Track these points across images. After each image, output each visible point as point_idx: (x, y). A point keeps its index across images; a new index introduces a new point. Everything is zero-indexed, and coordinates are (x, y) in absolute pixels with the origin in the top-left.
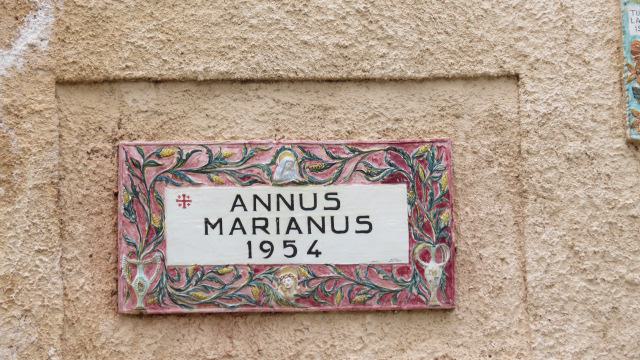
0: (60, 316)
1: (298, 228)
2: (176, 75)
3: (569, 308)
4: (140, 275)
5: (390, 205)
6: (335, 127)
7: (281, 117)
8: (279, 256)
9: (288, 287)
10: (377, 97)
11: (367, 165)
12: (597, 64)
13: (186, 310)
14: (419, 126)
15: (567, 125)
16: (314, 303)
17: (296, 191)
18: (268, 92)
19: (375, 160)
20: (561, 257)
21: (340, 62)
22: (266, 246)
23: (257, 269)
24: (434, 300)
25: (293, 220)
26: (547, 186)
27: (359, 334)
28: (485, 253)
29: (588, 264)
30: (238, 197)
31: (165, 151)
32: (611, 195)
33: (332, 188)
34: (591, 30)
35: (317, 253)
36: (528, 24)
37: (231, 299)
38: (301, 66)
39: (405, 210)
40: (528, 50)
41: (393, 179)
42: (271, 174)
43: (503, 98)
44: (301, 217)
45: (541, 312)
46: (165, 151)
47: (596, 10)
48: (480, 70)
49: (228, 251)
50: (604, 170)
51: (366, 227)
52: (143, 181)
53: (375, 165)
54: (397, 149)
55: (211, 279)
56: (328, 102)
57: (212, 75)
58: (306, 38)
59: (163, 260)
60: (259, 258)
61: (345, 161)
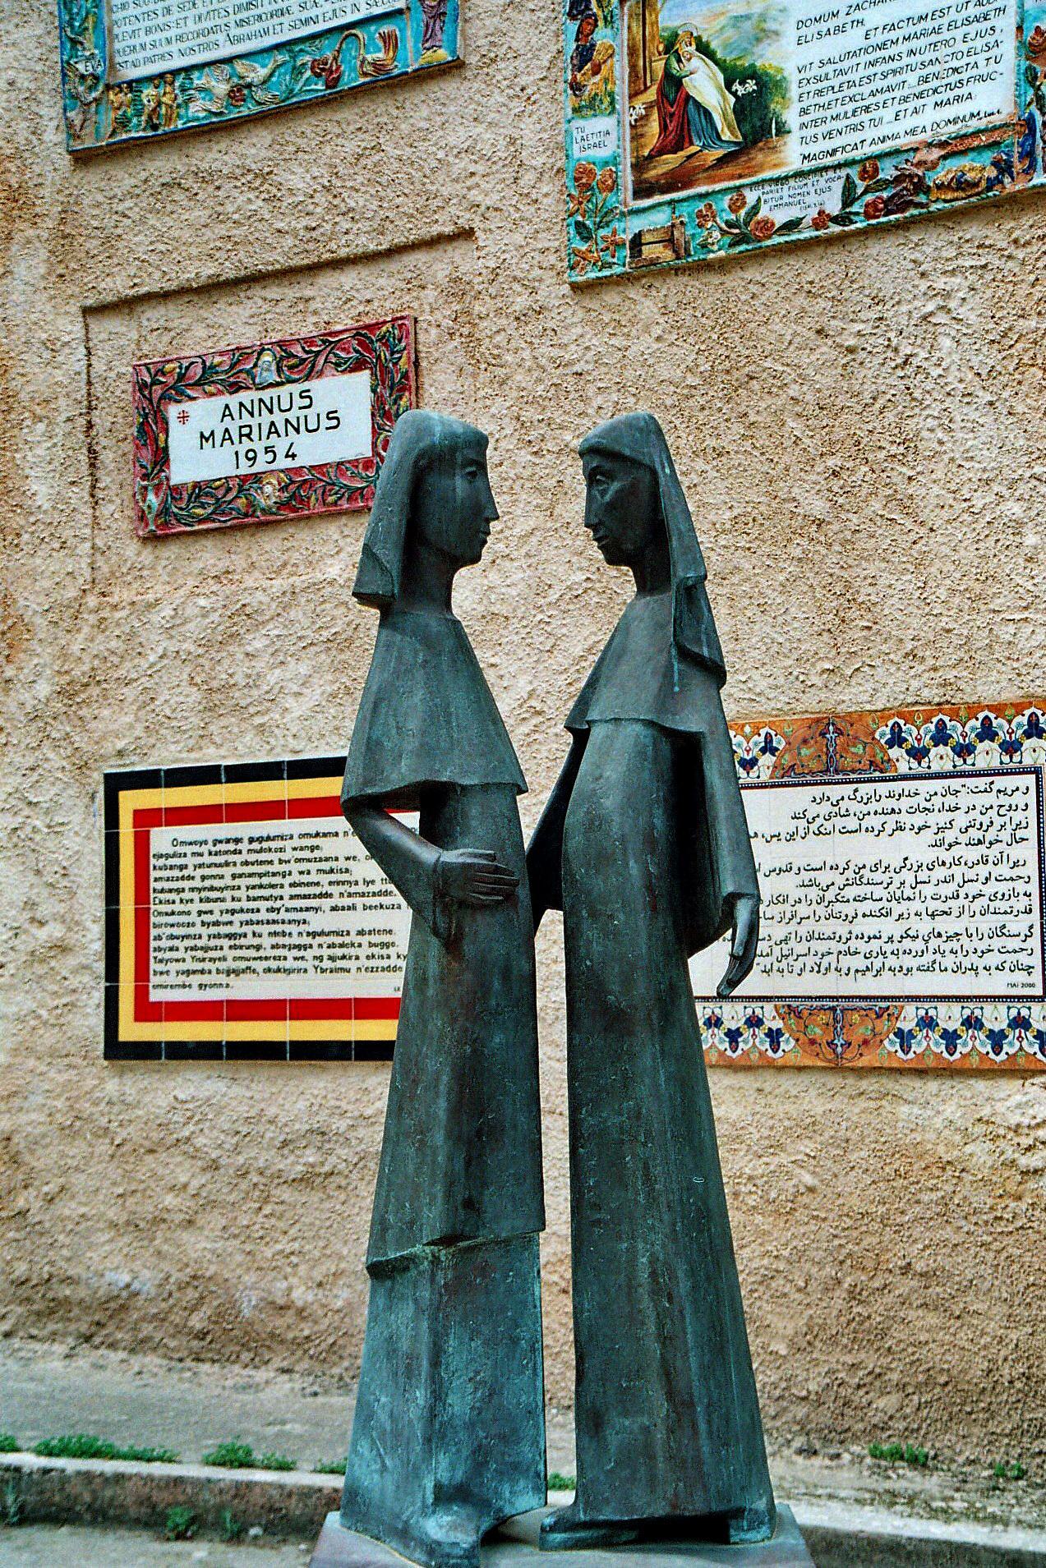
0: (88, 545)
1: (277, 432)
2: (173, 286)
3: (517, 487)
4: (151, 497)
6: (314, 319)
7: (268, 316)
9: (268, 496)
10: (348, 278)
11: (336, 355)
12: (545, 201)
13: (189, 529)
14: (387, 304)
15: (515, 278)
16: (295, 510)
18: (257, 291)
19: (343, 350)
20: (508, 431)
21: (311, 246)
22: (251, 455)
23: (244, 479)
25: (273, 424)
26: (496, 352)
27: (335, 537)
29: (533, 435)
30: (227, 407)
31: (169, 367)
32: (555, 352)
33: (306, 385)
34: (538, 161)
35: (294, 456)
36: (480, 168)
37: (223, 513)
38: (276, 259)
40: (480, 198)
41: (358, 366)
42: (253, 379)
43: (461, 258)
44: (278, 418)
46: (169, 367)
47: (545, 136)
48: (436, 230)
49: (217, 464)
50: (550, 324)
51: (334, 422)
52: (151, 402)
53: (343, 355)
54: (364, 334)
55: (207, 495)
56: (308, 293)
57: (203, 281)
58: (280, 225)
59: (168, 479)
60: (245, 469)
61: (318, 353)
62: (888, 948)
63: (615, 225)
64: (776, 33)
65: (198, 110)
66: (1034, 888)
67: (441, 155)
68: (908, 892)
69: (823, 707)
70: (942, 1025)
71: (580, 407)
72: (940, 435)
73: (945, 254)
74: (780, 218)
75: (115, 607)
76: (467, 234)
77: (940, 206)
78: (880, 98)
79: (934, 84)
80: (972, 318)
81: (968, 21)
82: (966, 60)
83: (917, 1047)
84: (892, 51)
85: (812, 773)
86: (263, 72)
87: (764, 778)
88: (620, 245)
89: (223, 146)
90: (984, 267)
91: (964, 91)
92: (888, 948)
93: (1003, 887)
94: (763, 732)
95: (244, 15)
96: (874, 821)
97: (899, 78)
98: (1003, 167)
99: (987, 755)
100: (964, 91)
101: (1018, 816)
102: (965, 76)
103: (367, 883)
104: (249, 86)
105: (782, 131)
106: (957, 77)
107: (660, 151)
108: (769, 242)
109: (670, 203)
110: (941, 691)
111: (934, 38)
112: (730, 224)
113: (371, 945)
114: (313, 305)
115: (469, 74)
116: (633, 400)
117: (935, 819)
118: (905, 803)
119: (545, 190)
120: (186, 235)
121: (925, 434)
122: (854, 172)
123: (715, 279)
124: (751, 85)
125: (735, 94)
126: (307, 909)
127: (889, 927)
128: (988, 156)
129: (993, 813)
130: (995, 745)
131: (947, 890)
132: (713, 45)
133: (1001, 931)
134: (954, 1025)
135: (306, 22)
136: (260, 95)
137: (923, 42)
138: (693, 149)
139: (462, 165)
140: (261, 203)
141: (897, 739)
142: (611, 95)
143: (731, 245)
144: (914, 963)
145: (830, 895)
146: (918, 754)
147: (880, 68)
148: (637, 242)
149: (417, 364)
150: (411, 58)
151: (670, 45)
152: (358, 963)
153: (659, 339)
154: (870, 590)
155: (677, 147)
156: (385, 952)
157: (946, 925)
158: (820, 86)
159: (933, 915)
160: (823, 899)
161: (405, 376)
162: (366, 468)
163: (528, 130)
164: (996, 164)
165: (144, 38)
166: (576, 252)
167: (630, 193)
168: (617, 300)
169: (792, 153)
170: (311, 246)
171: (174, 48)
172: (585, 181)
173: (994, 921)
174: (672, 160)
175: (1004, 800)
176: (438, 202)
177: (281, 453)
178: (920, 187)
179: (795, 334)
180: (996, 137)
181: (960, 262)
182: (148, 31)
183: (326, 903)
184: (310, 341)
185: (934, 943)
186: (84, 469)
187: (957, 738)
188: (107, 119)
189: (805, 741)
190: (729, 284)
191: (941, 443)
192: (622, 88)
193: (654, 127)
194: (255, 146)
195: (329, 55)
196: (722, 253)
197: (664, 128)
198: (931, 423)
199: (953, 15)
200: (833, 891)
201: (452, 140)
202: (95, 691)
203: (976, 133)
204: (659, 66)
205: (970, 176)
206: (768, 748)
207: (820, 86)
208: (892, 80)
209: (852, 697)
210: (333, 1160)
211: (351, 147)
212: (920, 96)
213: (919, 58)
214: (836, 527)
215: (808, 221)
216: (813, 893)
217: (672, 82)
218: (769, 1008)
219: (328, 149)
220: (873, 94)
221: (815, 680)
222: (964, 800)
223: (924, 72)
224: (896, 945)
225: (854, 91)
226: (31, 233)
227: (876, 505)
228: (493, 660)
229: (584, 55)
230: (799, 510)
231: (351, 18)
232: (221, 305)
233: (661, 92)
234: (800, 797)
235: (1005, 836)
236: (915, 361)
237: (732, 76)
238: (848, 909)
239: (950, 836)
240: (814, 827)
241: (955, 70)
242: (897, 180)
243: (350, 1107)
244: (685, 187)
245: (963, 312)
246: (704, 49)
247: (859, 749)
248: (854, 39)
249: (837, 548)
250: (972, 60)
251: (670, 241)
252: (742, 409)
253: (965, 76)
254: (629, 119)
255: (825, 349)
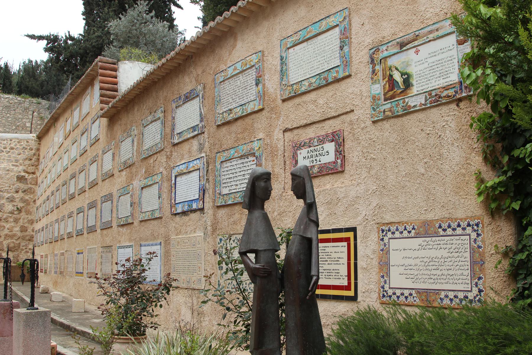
2: (298, 126)
5: (330, 147)
6: (324, 131)
8: (314, 164)
9: (315, 170)
10: (331, 122)
16: (321, 173)
17: (317, 147)
18: (314, 126)
21: (323, 115)
24: (340, 169)
28: (350, 156)
31: (298, 143)
32: (369, 136)
36: (354, 97)
38: (317, 119)
39: (334, 148)
41: (332, 141)
43: (351, 116)
44: (318, 153)
45: (357, 169)
46: (298, 143)
47: (367, 89)
48: (347, 110)
50: (368, 130)
54: (333, 133)
57: (304, 124)
58: (318, 111)
60: (312, 164)
62: (438, 277)
63: (380, 107)
64: (411, 65)
65: (303, 89)
66: (469, 264)
67: (347, 94)
68: (443, 264)
69: (425, 219)
70: (450, 297)
71: (375, 148)
72: (447, 153)
73: (447, 112)
74: (412, 105)
75: (288, 195)
76: (353, 111)
77: (445, 101)
78: (432, 78)
79: (442, 74)
80: (453, 126)
81: (448, 61)
82: (448, 69)
83: (444, 302)
84: (434, 67)
85: (422, 234)
86: (315, 80)
87: (413, 236)
88: (381, 112)
89: (308, 96)
90: (455, 114)
91: (448, 76)
92: (438, 277)
93: (463, 263)
94: (412, 225)
95: (312, 69)
96: (435, 246)
97: (435, 73)
98: (456, 92)
99: (459, 231)
100: (448, 76)
101: (466, 246)
102: (448, 72)
103: (335, 258)
104: (312, 83)
105: (412, 86)
106: (447, 73)
107: (389, 91)
108: (410, 110)
109: (391, 102)
110: (449, 215)
111: (442, 64)
112: (403, 107)
113: (335, 273)
114: (325, 128)
115: (352, 77)
116: (385, 147)
117: (449, 246)
118: (442, 242)
119: (367, 101)
120: (301, 115)
121: (444, 153)
122: (427, 94)
123: (400, 119)
124: (406, 76)
125: (403, 78)
126: (323, 264)
127: (438, 272)
128: (453, 90)
129: (460, 245)
130: (461, 228)
131: (451, 264)
132: (398, 68)
133: (462, 274)
134: (452, 297)
135: (322, 69)
136: (314, 85)
137: (440, 65)
138: (395, 90)
139: (351, 96)
140: (314, 107)
141: (440, 227)
142: (379, 80)
143: (403, 111)
144: (444, 281)
145: (426, 264)
146: (444, 230)
147: (431, 71)
148: (384, 111)
149: (344, 140)
150: (341, 75)
151: (390, 69)
152: (333, 277)
153: (389, 133)
154: (434, 191)
155: (392, 90)
156: (338, 274)
157: (451, 272)
158: (420, 75)
159: (448, 270)
160: (425, 265)
161: (341, 143)
162: (334, 163)
163: (364, 89)
164: (455, 91)
165: (294, 76)
166: (373, 114)
167: (383, 100)
168: (381, 124)
169: (415, 90)
170: (323, 115)
171: (300, 76)
172: (374, 98)
173: (460, 272)
174: (391, 93)
175: (463, 242)
176: (347, 104)
177: (318, 161)
178: (440, 97)
179: (417, 131)
180: (454, 86)
181: (450, 114)
182: (295, 74)
183: (327, 263)
184: (323, 136)
185: (448, 276)
186: (283, 165)
187: (453, 227)
188: (287, 92)
189: (421, 227)
190: (403, 120)
191: (448, 155)
192: (381, 78)
193: (387, 86)
194: (312, 96)
195: (326, 75)
196: (401, 113)
197: (389, 86)
198: (446, 151)
199: (445, 59)
200: (427, 263)
201: (349, 91)
202: (284, 214)
203: (451, 85)
204: (388, 73)
205: (450, 94)
206: (413, 228)
207: (420, 75)
208: (434, 74)
209: (430, 216)
210: (328, 322)
211: (331, 94)
212: (439, 77)
213: (439, 69)
214: (426, 176)
215: (418, 105)
216: (423, 263)
217: (391, 76)
218: (414, 291)
219: (326, 95)
220: (430, 77)
221: (423, 212)
222: (454, 242)
223: (440, 72)
224: (440, 277)
225: (426, 76)
226: (275, 116)
227: (435, 170)
228: (358, 207)
229: (374, 72)
230: (419, 172)
231: (330, 68)
232: (308, 129)
233: (389, 78)
234: (420, 240)
235: (463, 251)
236: (442, 136)
237: (402, 74)
238: (430, 268)
239: (451, 250)
240: (423, 248)
241: (446, 71)
242: (436, 95)
243: (331, 310)
244: (394, 98)
245: (451, 125)
246: (397, 69)
247: (432, 229)
248: (426, 65)
249: (427, 181)
250: (449, 69)
251: (390, 111)
252: (407, 148)
253: (448, 72)
254: (383, 84)
255: (423, 134)
